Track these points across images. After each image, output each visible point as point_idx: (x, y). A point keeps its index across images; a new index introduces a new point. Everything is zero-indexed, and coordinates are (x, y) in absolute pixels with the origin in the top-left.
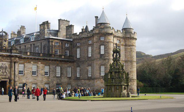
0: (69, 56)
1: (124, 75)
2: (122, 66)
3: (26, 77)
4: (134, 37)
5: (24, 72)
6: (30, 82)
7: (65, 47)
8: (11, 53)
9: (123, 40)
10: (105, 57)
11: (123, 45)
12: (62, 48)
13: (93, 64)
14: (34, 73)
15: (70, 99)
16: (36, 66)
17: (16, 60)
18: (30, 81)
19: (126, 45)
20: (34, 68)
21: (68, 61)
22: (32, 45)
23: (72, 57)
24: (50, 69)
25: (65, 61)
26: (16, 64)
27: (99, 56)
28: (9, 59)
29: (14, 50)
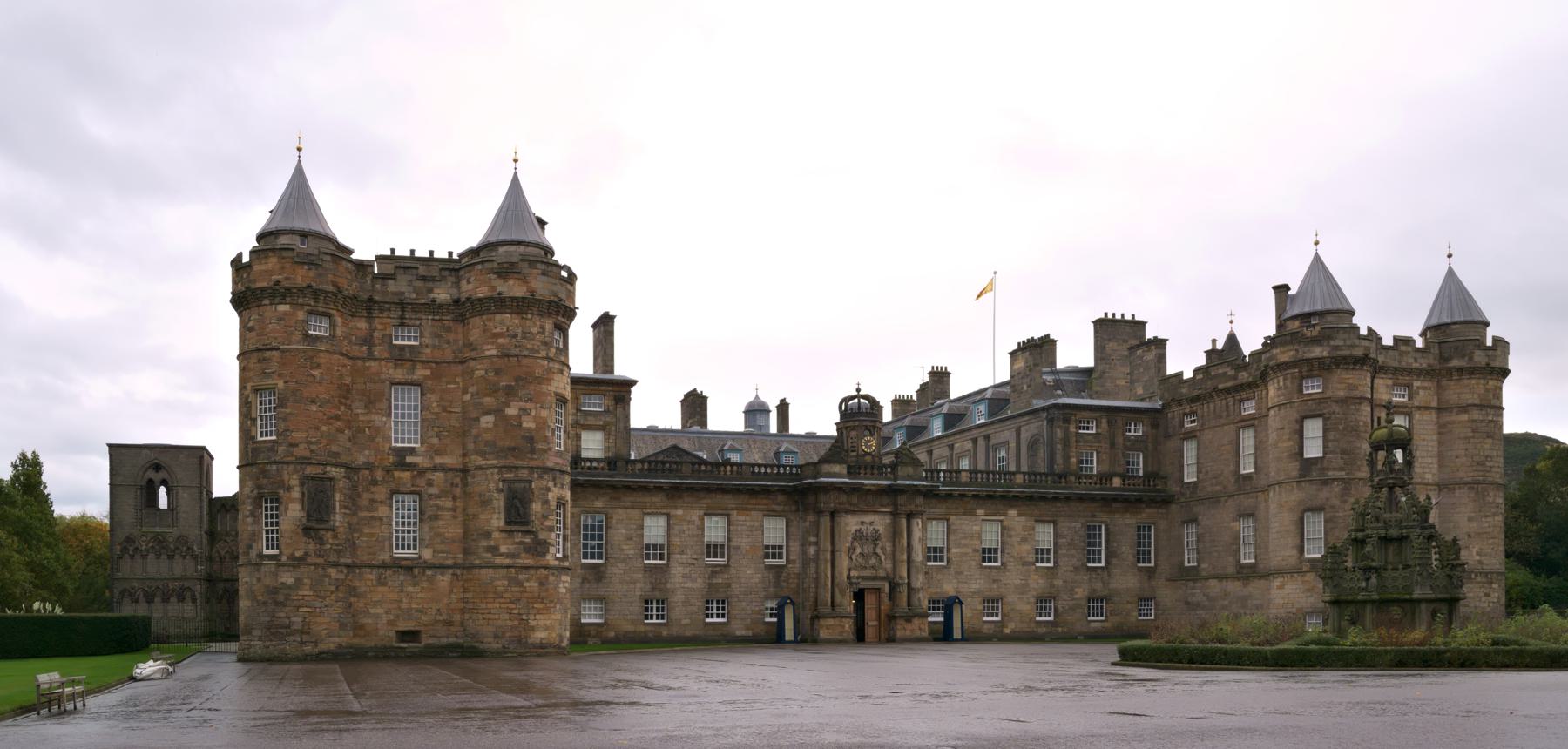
1: (1434, 550)
2: (1425, 512)
4: (1493, 365)
5: (948, 551)
8: (895, 479)
9: (1426, 384)
10: (1328, 469)
11: (1427, 408)
13: (1263, 506)
14: (987, 554)
16: (996, 528)
17: (913, 507)
19: (1439, 410)
20: (991, 535)
22: (981, 442)
24: (1056, 535)
25: (1126, 500)
27: (1293, 468)
28: (885, 500)
29: (906, 464)
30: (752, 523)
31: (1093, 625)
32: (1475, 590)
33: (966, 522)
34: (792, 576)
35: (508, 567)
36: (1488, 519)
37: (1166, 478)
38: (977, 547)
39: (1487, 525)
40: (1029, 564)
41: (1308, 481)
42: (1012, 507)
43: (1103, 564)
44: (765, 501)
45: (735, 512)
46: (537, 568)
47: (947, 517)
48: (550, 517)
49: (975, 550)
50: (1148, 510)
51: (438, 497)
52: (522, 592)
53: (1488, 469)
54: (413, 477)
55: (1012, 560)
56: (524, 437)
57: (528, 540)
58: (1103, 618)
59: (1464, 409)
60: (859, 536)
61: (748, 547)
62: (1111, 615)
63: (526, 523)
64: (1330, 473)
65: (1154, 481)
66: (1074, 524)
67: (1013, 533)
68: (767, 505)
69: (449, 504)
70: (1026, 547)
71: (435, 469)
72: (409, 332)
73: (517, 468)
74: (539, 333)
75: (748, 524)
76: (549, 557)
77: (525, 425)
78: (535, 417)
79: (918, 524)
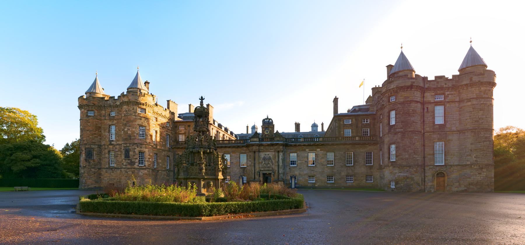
0: (370, 136)
3: (300, 168)
6: (305, 174)
7: (363, 124)
10: (397, 129)
12: (357, 127)
15: (61, 198)
17: (279, 149)
18: (305, 172)
21: (365, 144)
23: (373, 137)
24: (335, 156)
26: (280, 153)
30: (236, 156)
31: (348, 184)
32: (474, 172)
33: (303, 153)
34: (248, 170)
35: (125, 168)
36: (480, 143)
37: (377, 136)
38: (306, 161)
39: (480, 146)
40: (324, 165)
41: (390, 133)
42: (318, 148)
43: (352, 165)
44: (240, 150)
45: (232, 153)
46: (131, 168)
47: (296, 152)
49: (305, 162)
50: (369, 147)
51: (118, 152)
52: (128, 175)
53: (481, 123)
54: (113, 147)
55: (318, 164)
56: (128, 136)
57: (129, 162)
58: (353, 182)
59: (469, 100)
60: (264, 159)
61: (235, 163)
62: (355, 181)
63: (129, 157)
64: (397, 130)
65: (372, 137)
66: (341, 153)
67: (319, 156)
68: (240, 151)
69: (120, 153)
70: (323, 160)
71: (117, 145)
72: (92, 112)
73: (126, 143)
75: (235, 156)
76: (135, 166)
77: (128, 133)
78: (131, 130)
79: (281, 155)
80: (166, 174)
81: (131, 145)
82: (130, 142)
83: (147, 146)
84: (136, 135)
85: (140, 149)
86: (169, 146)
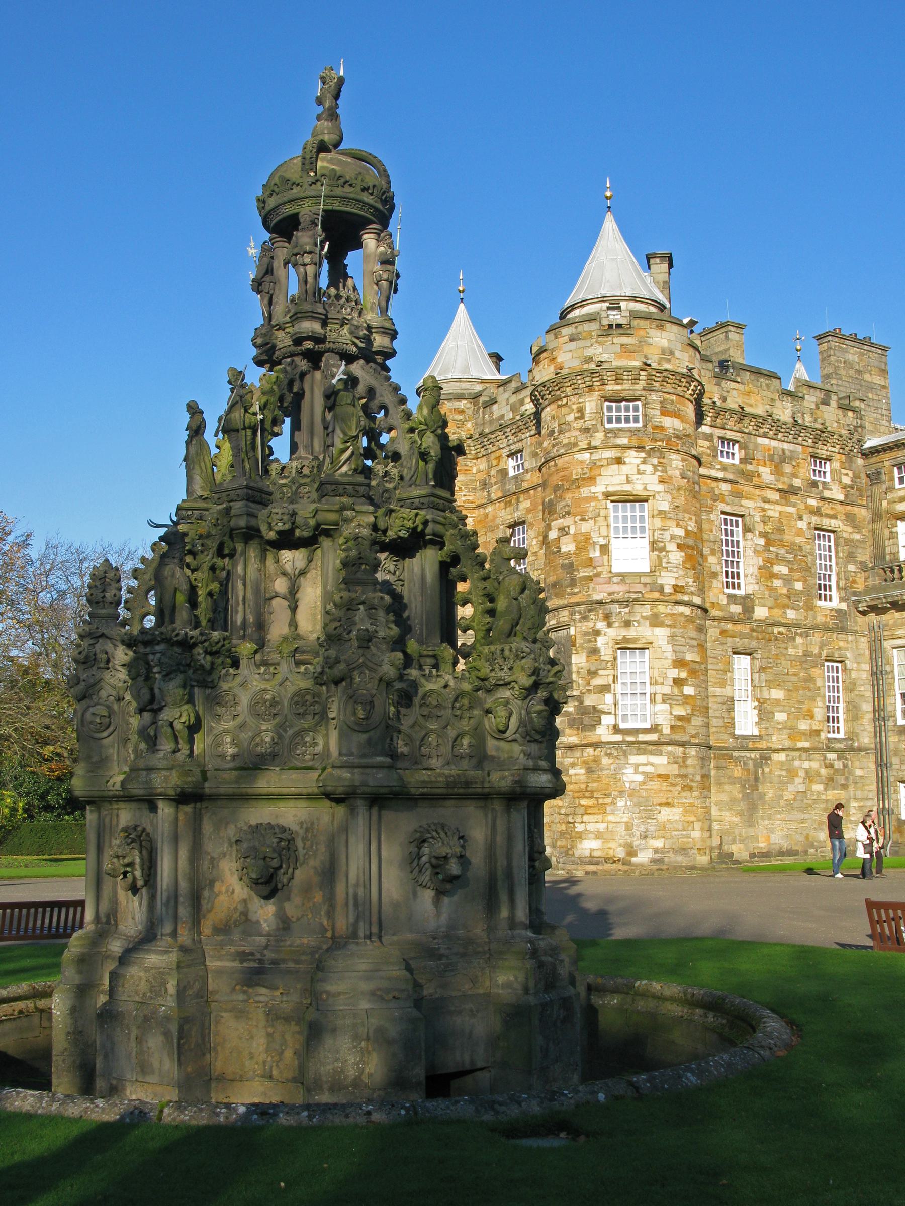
48: (601, 672)
74: (576, 418)
77: (564, 549)
80: (823, 771)
81: (578, 616)
82: (575, 599)
83: (662, 608)
84: (597, 554)
85: (624, 632)
86: (842, 600)
